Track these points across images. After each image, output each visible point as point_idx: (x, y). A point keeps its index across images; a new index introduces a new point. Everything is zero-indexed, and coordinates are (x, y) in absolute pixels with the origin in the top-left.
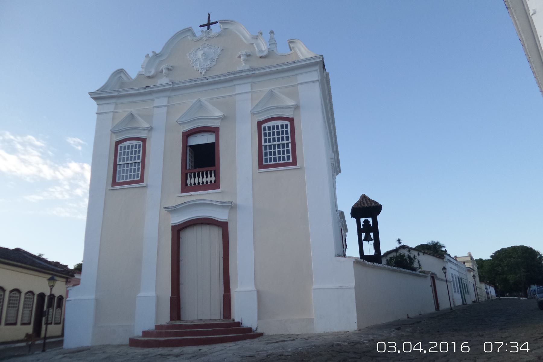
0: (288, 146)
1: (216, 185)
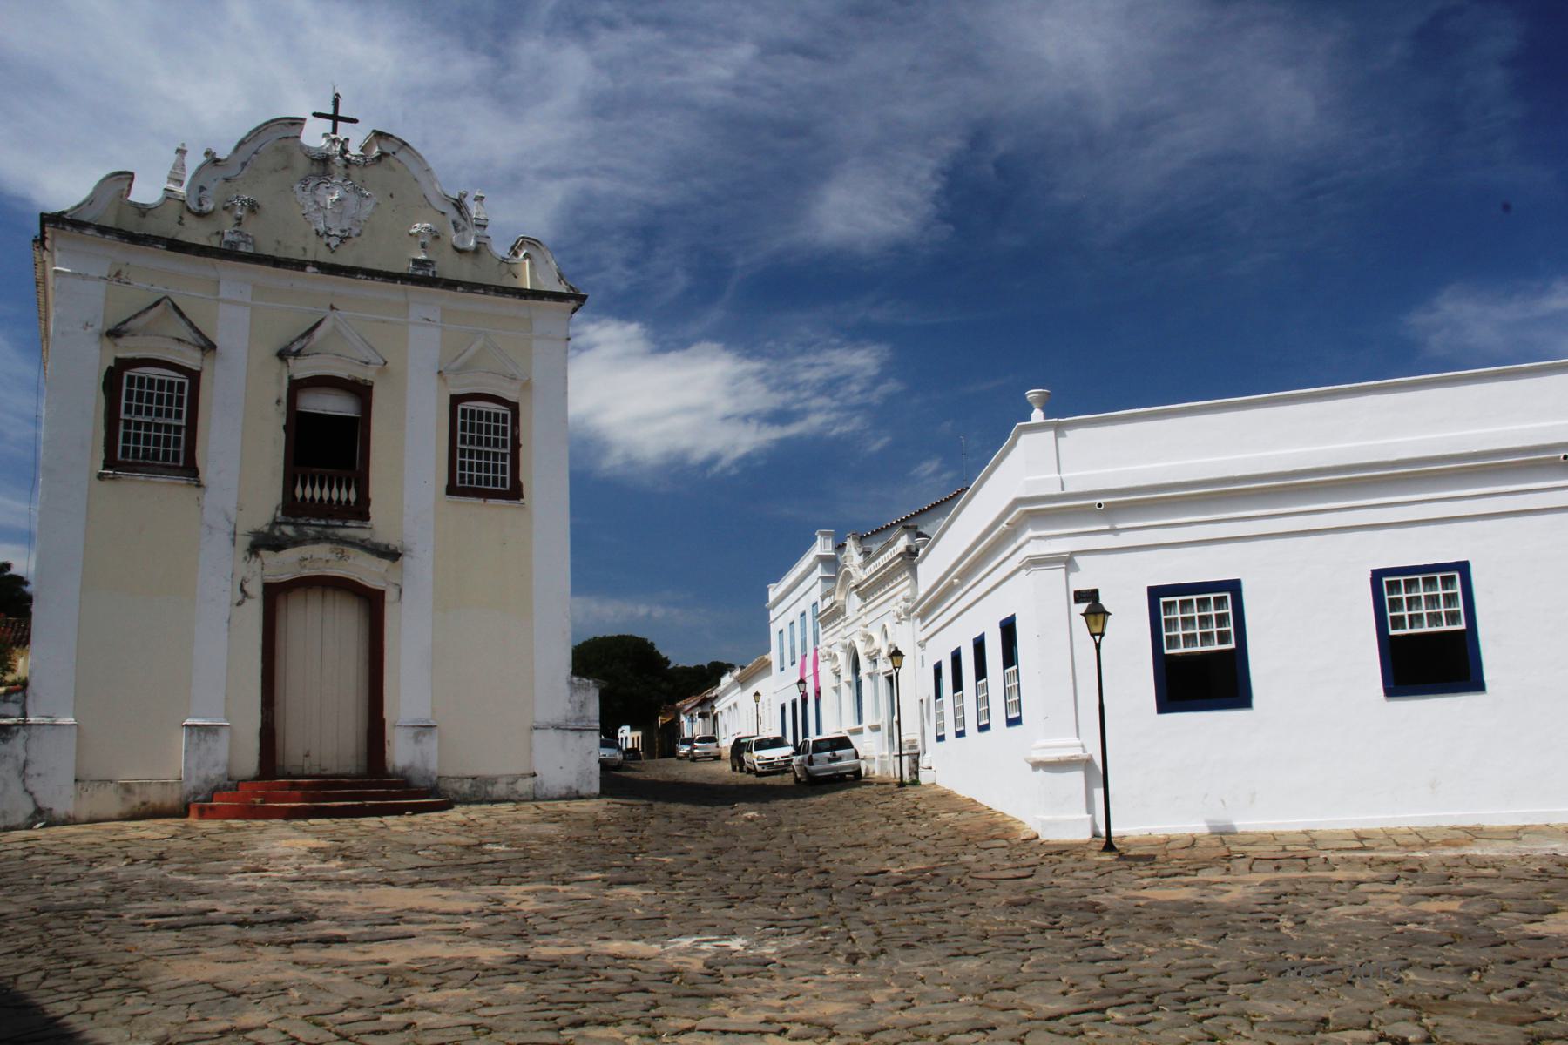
0: (504, 459)
1: (360, 511)
